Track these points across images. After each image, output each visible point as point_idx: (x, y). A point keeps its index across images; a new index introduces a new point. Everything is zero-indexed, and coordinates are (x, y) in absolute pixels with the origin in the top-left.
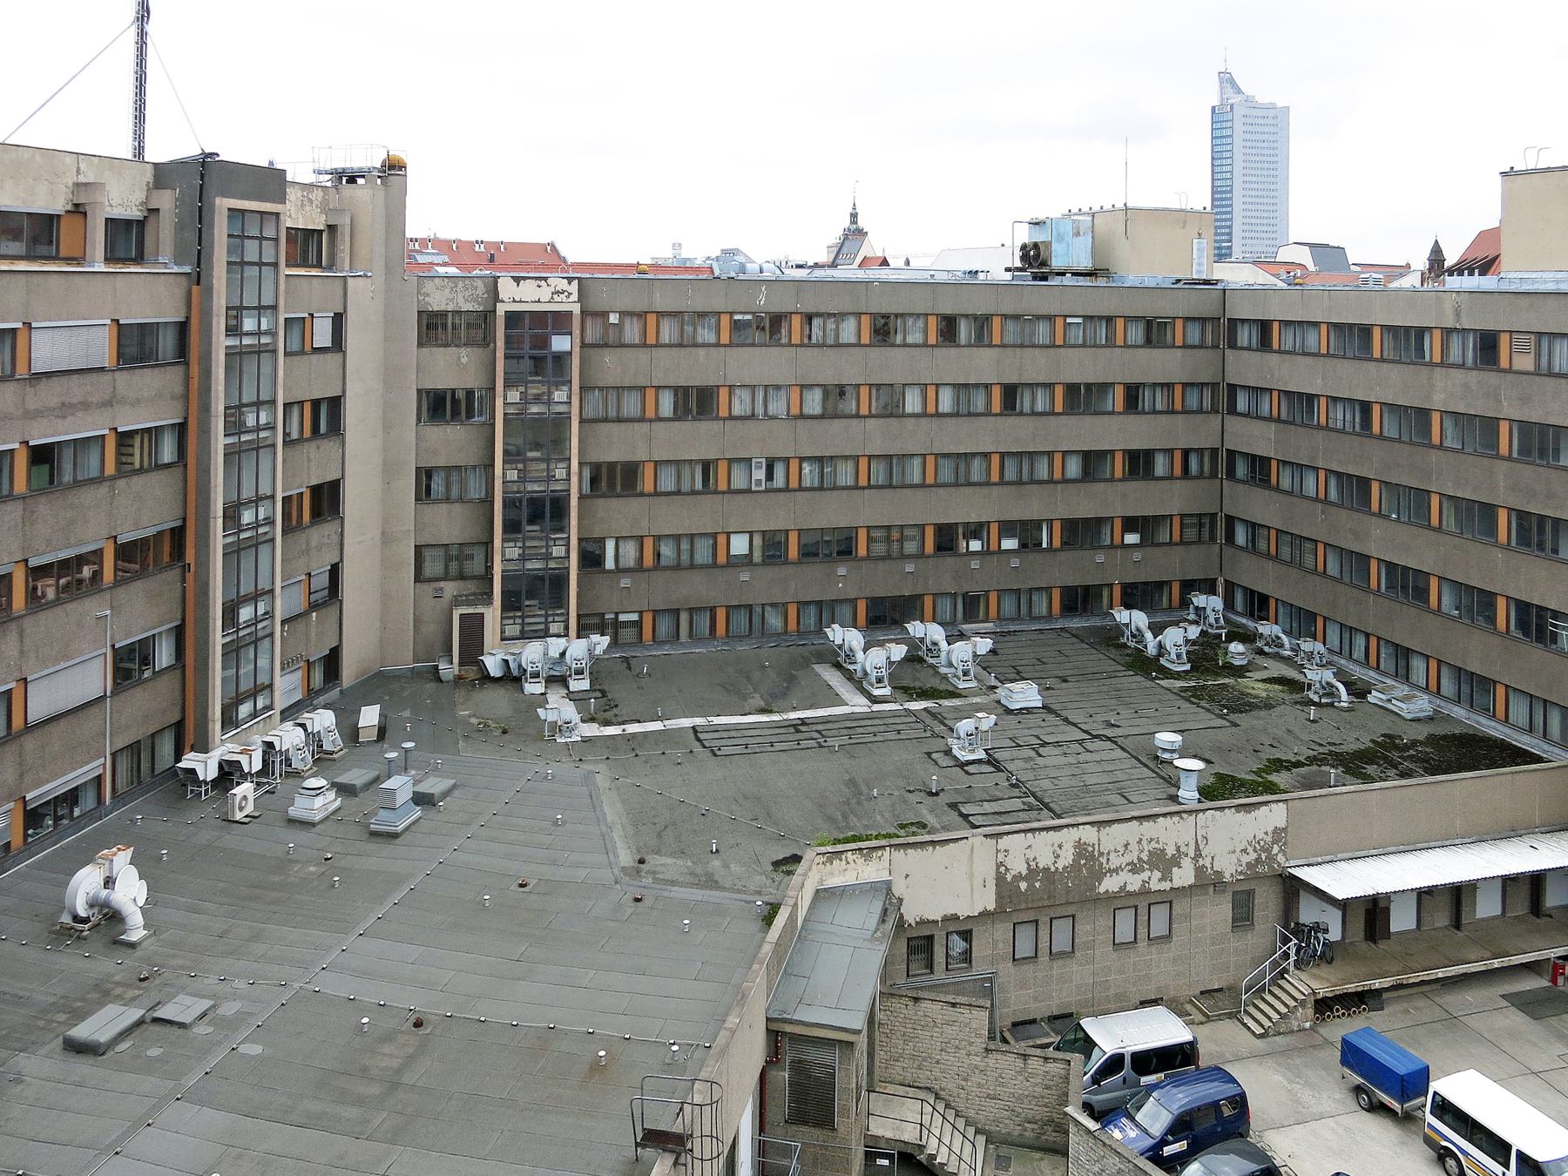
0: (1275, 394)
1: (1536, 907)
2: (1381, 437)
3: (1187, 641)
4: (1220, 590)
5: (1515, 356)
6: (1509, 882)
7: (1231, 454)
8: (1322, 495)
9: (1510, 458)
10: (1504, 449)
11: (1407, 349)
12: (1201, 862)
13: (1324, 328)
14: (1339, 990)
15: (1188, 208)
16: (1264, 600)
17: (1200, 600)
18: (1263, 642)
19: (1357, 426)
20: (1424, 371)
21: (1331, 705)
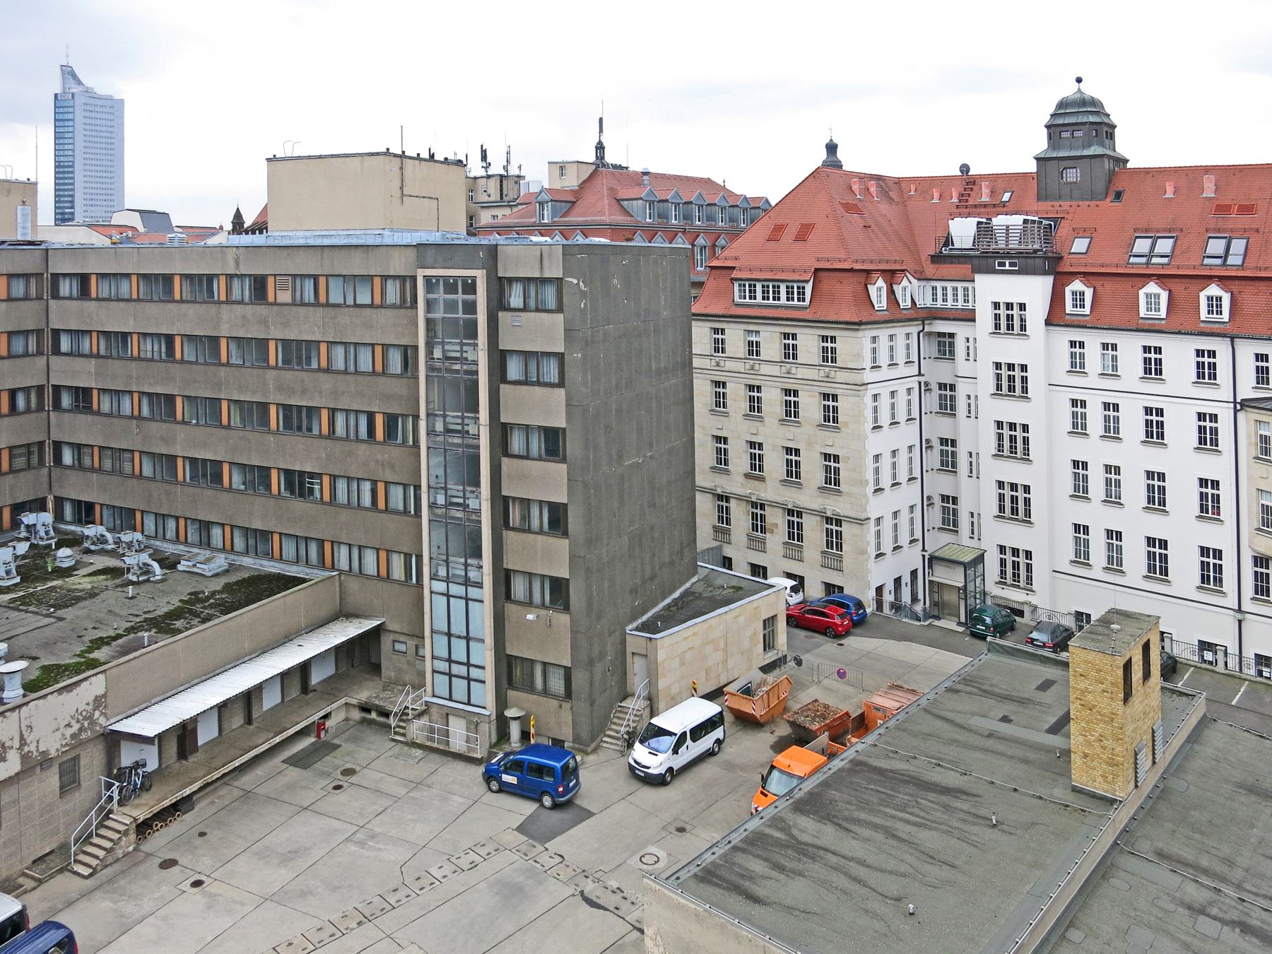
0: (94, 335)
1: (305, 689)
2: (182, 361)
3: (16, 558)
4: (50, 505)
5: (278, 292)
6: (284, 676)
7: (57, 389)
8: (136, 413)
9: (276, 368)
10: (272, 362)
11: (201, 291)
12: (26, 749)
13: (134, 278)
14: (156, 809)
15: (13, 179)
16: (90, 507)
17: (29, 518)
18: (89, 542)
19: (163, 355)
20: (212, 309)
21: (148, 581)
